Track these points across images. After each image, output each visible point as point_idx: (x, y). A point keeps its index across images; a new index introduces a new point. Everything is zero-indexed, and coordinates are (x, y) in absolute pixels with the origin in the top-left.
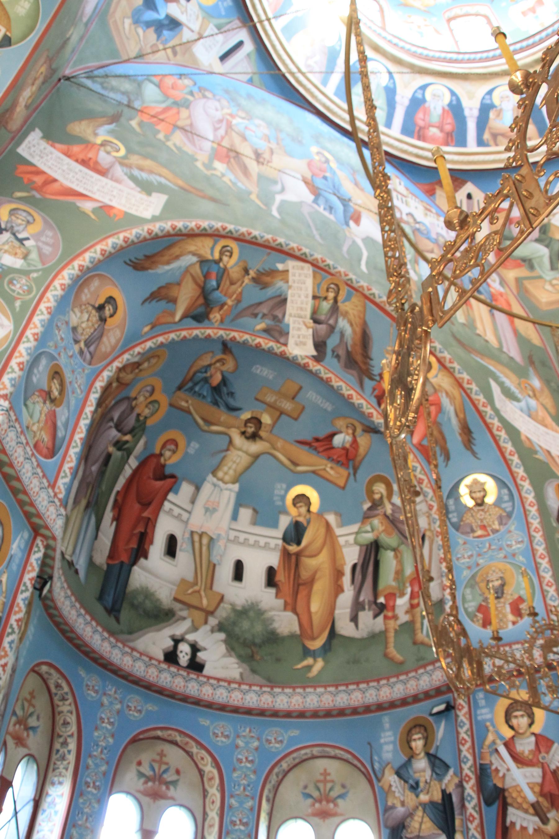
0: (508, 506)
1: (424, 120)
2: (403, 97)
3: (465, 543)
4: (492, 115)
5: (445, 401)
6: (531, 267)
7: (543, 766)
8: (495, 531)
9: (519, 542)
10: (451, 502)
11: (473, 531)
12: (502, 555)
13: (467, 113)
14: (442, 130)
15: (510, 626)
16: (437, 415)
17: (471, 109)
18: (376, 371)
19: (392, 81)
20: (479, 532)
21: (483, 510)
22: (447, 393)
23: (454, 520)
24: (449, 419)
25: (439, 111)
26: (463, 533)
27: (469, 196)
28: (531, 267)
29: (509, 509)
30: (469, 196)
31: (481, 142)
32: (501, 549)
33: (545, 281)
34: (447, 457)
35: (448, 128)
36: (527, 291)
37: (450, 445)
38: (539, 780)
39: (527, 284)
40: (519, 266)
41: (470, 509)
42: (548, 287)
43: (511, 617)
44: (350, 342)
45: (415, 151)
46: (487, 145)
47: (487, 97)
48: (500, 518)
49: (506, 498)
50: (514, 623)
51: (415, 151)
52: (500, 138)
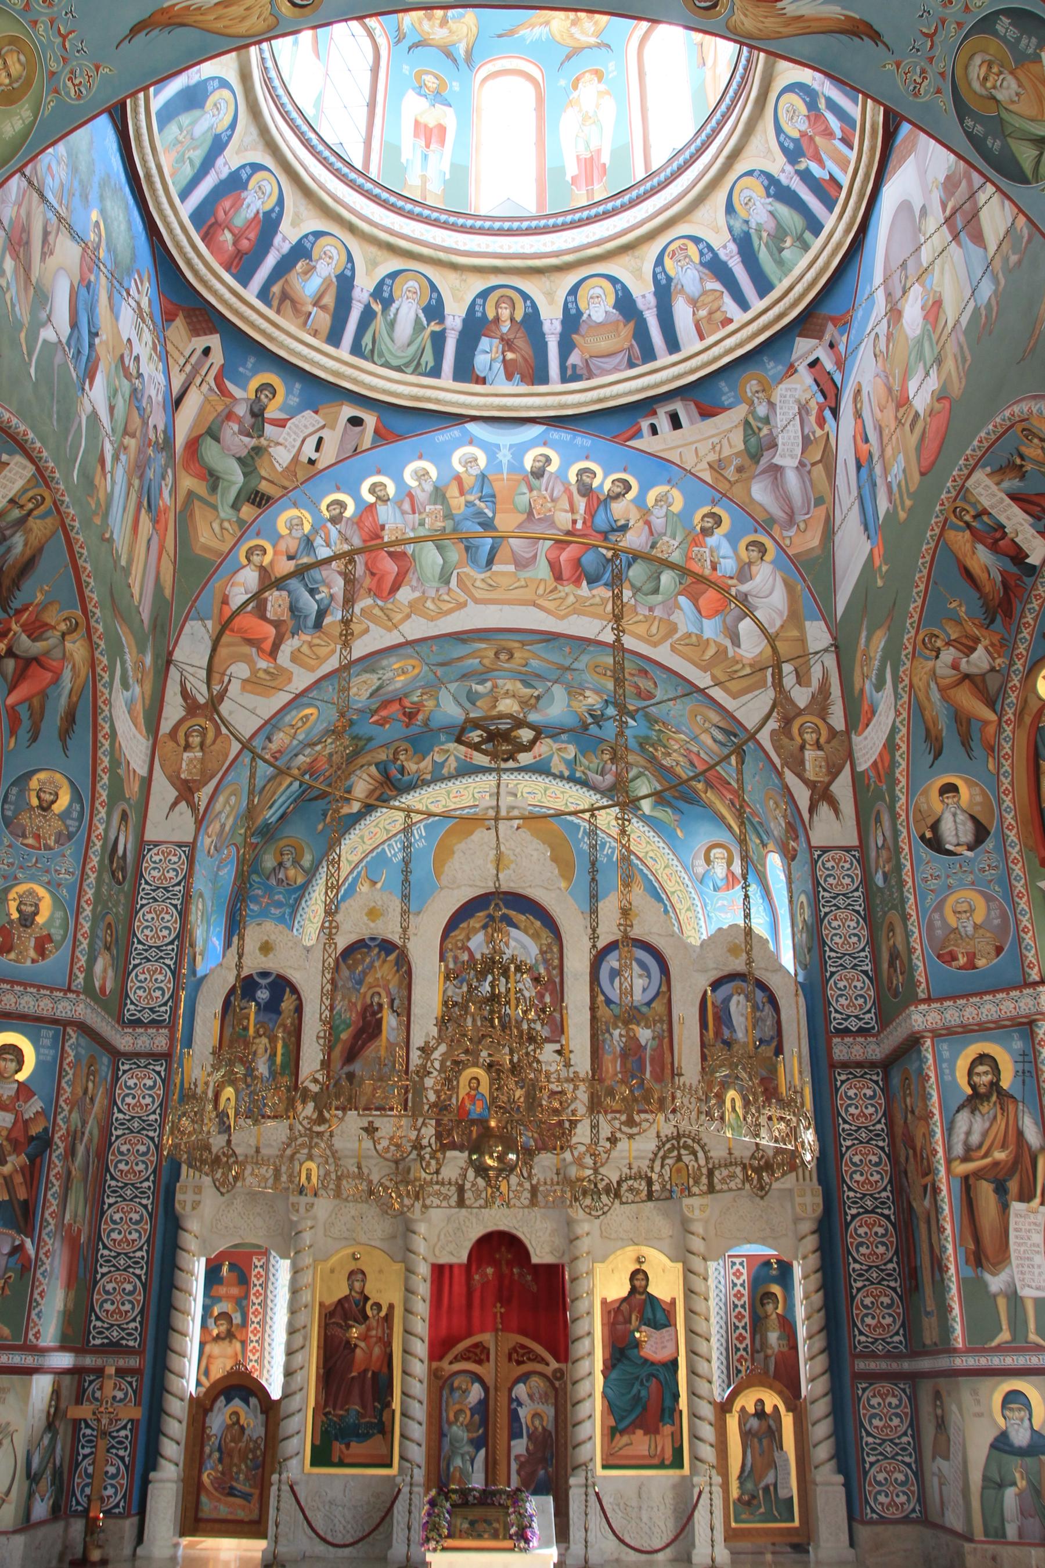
0: (73, 824)
1: (226, 213)
2: (226, 163)
3: (10, 846)
4: (300, 266)
5: (67, 674)
6: (214, 488)
7: (18, 1115)
8: (48, 848)
9: (67, 872)
10: (14, 790)
11: (24, 836)
12: (46, 879)
13: (277, 240)
14: (235, 243)
15: (29, 963)
16: (48, 686)
17: (284, 239)
18: (16, 604)
19: (229, 133)
20: (30, 841)
21: (44, 817)
22: (74, 666)
23: (9, 813)
24: (60, 695)
25: (251, 214)
26: (11, 833)
27: (207, 351)
28: (214, 488)
29: (71, 829)
30: (207, 351)
31: (264, 294)
32: (47, 871)
33: (218, 516)
34: (34, 738)
35: (245, 244)
36: (192, 514)
37: (44, 726)
38: (9, 1126)
39: (197, 503)
40: (202, 478)
41: (33, 808)
42: (216, 526)
43: (32, 953)
44: (10, 561)
45: (192, 254)
46: (268, 303)
47: (311, 238)
48: (59, 835)
49: (75, 815)
50: (33, 961)
51: (192, 254)
52: (288, 303)
